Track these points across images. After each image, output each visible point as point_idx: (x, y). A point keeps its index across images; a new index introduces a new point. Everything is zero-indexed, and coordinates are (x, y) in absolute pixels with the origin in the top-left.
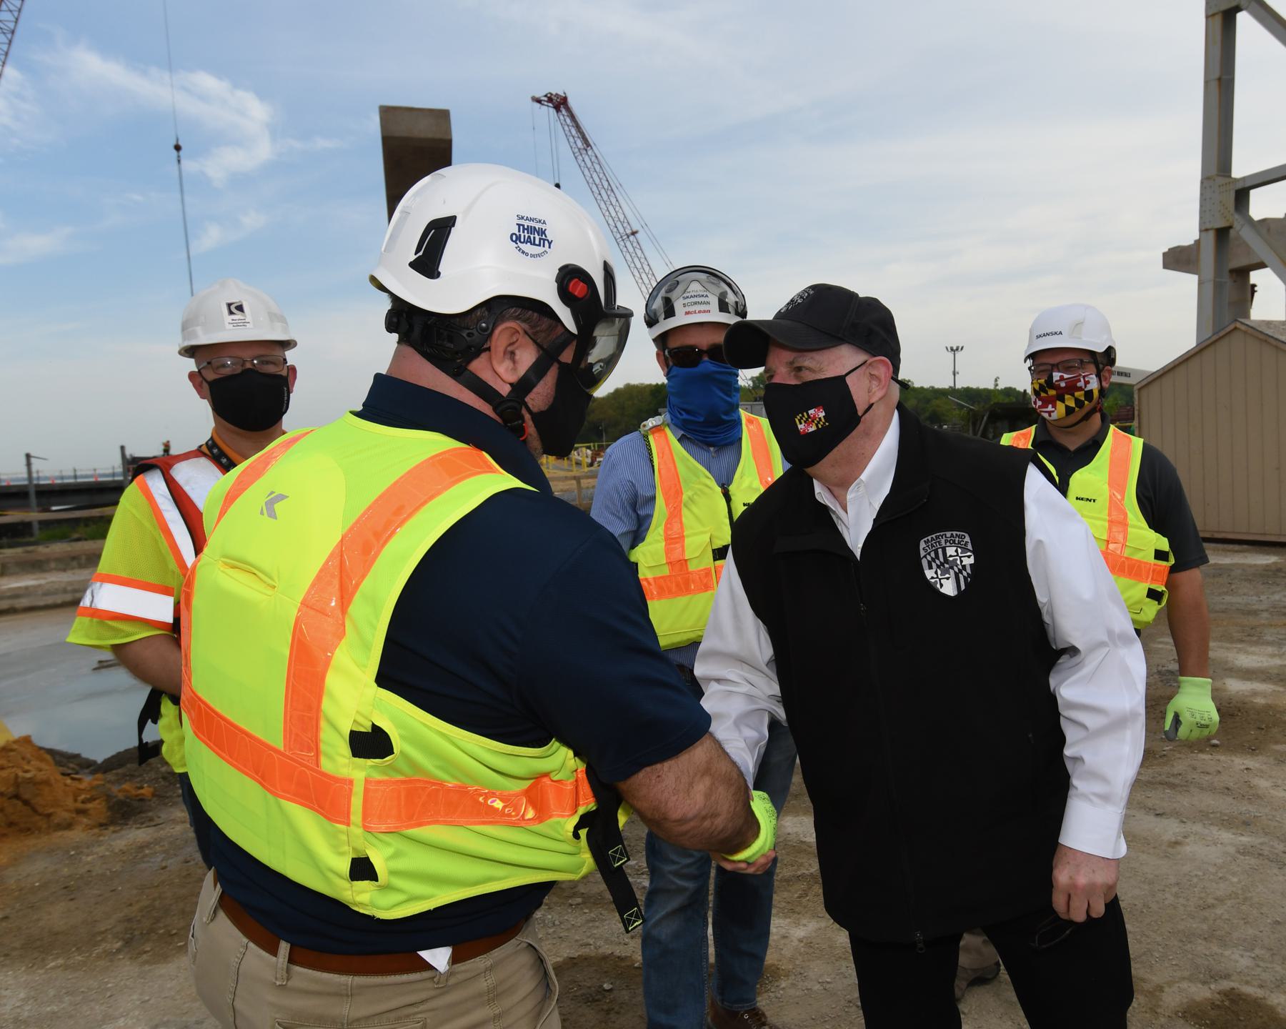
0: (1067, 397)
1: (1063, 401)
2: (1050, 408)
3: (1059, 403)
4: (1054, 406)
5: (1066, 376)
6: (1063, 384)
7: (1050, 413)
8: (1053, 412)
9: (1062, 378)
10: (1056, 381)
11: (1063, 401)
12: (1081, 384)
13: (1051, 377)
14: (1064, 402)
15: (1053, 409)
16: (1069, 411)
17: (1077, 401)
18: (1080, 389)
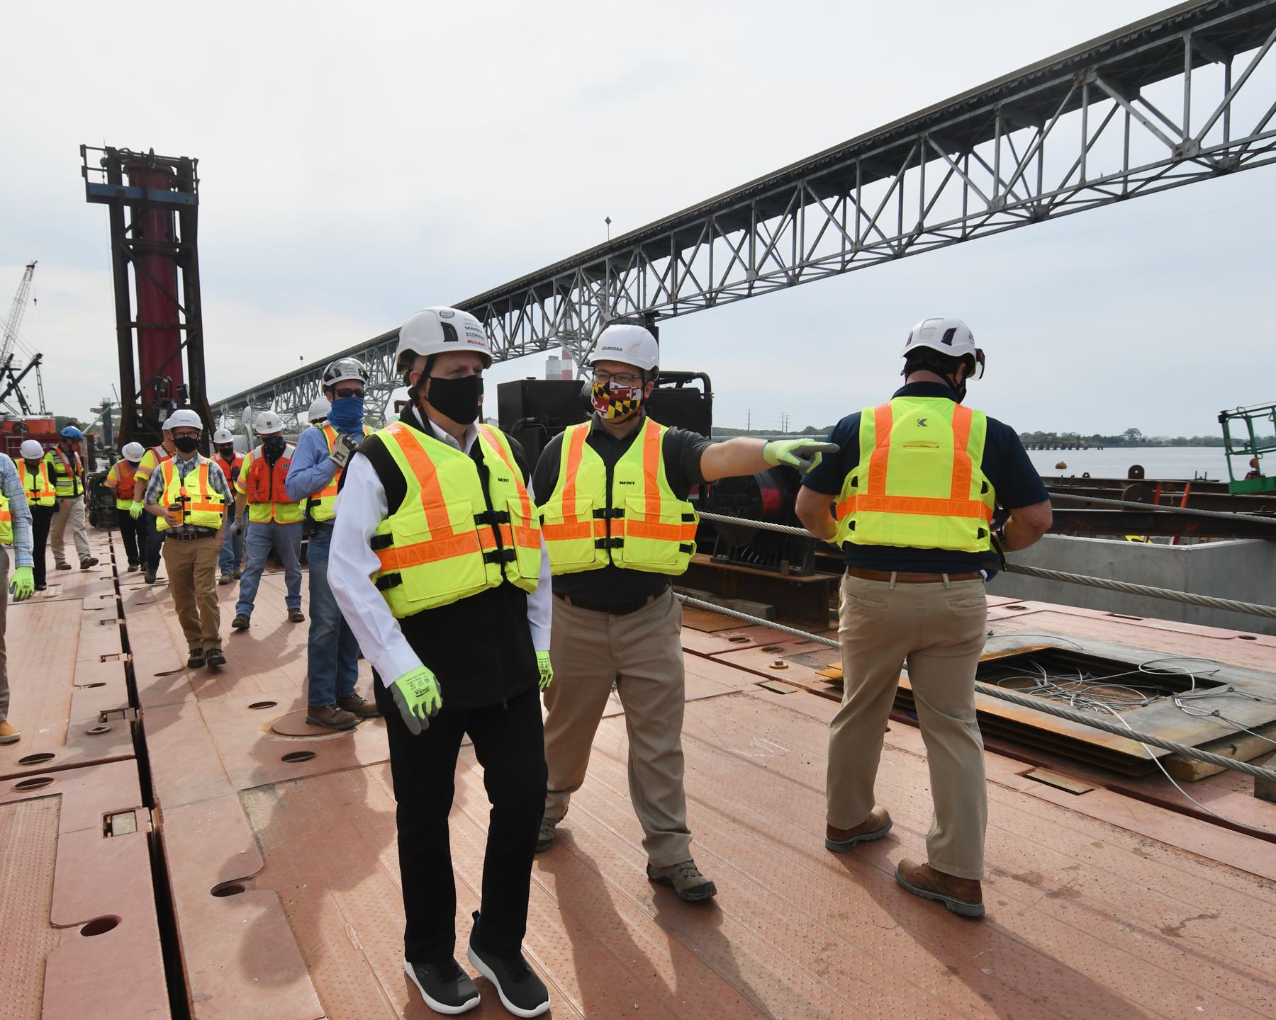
0: (618, 403)
5: (620, 386)
6: (616, 392)
9: (616, 388)
12: (629, 395)
17: (624, 407)
18: (628, 399)
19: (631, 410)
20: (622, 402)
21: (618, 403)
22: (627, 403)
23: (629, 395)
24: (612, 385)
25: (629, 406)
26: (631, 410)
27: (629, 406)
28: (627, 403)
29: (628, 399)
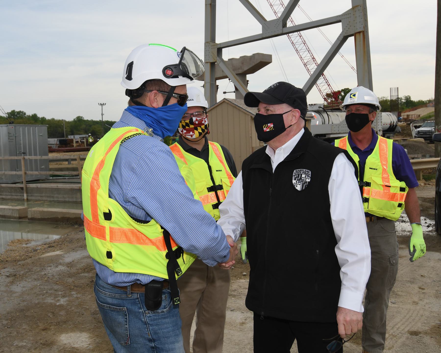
0: (199, 128)
1: (197, 130)
2: (191, 133)
3: (195, 131)
4: (194, 132)
5: (198, 119)
6: (197, 123)
7: (192, 136)
8: (194, 135)
9: (197, 120)
10: (195, 121)
11: (197, 130)
12: (203, 122)
13: (191, 120)
14: (197, 131)
15: (193, 134)
16: (200, 134)
17: (202, 130)
18: (203, 124)
19: (206, 130)
20: (201, 127)
21: (199, 128)
22: (203, 127)
23: (203, 122)
24: (194, 119)
25: (204, 128)
26: (206, 130)
27: (204, 128)
28: (203, 127)
29: (203, 124)
